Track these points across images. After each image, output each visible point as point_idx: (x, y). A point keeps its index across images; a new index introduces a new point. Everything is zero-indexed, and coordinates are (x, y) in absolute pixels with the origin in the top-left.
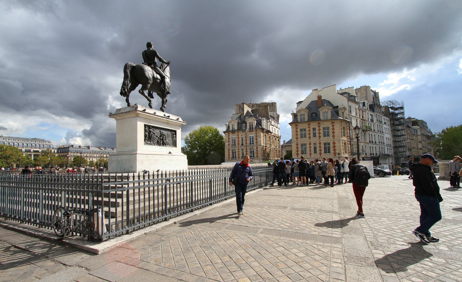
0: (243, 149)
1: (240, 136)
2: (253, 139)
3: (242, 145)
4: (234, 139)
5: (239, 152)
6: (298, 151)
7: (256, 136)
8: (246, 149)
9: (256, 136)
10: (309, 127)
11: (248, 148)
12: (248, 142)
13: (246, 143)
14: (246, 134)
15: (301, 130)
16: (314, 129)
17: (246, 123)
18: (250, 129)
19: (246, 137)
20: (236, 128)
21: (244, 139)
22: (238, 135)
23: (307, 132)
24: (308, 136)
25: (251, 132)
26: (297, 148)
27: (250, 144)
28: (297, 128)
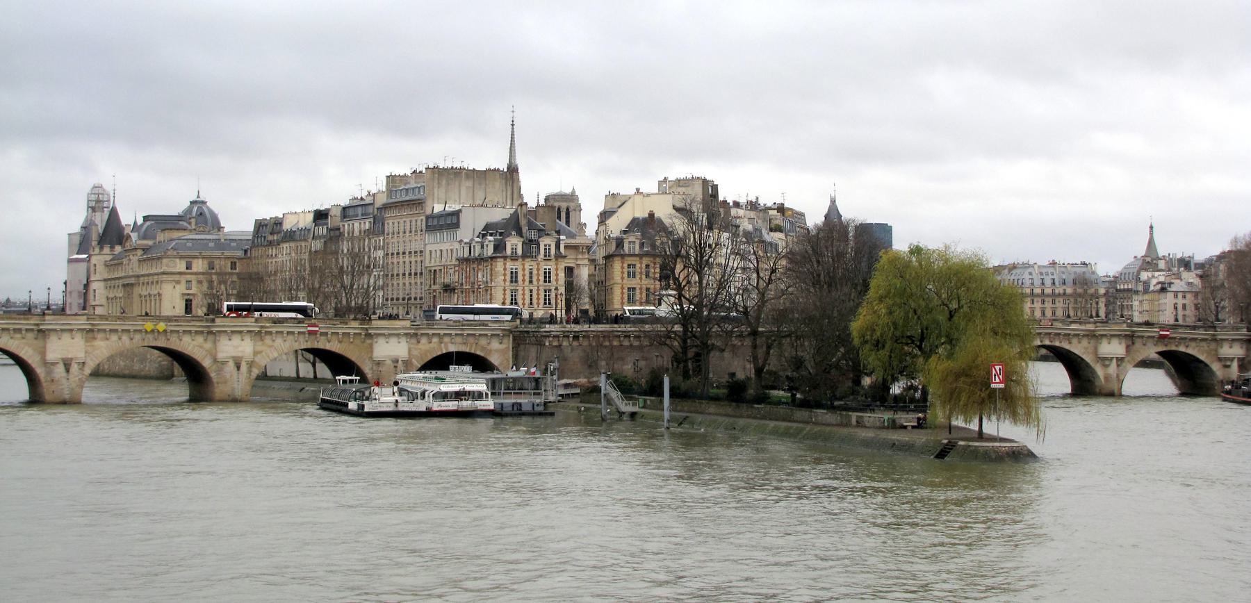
0: (531, 291)
1: (527, 267)
2: (550, 273)
3: (531, 282)
4: (514, 270)
5: (524, 294)
6: (622, 298)
7: (557, 269)
8: (538, 290)
9: (557, 269)
10: (641, 263)
11: (540, 288)
12: (542, 278)
13: (538, 280)
14: (538, 264)
15: (629, 266)
16: (647, 266)
17: (538, 244)
18: (545, 256)
19: (538, 270)
20: (520, 252)
21: (535, 272)
22: (523, 265)
23: (638, 270)
24: (638, 277)
25: (549, 263)
26: (622, 293)
27: (545, 282)
28: (623, 263)
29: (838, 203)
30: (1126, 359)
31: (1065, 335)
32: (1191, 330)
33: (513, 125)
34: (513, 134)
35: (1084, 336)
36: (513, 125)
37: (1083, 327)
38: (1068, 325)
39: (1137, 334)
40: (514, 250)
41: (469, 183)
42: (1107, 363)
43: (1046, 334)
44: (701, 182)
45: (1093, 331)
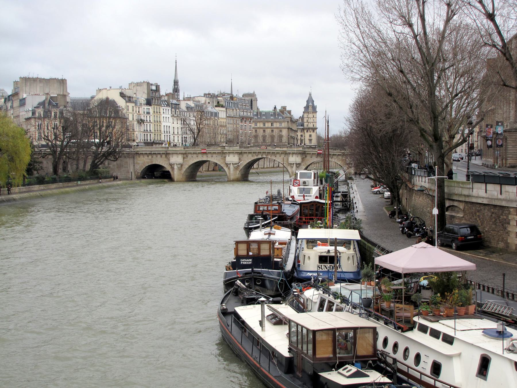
29: (312, 95)
30: (302, 164)
31: (273, 153)
32: (333, 150)
33: (176, 62)
34: (176, 66)
35: (281, 153)
36: (176, 62)
37: (281, 149)
38: (274, 148)
39: (307, 152)
40: (40, 114)
41: (42, 85)
42: (292, 166)
43: (263, 152)
44: (146, 84)
45: (286, 151)
